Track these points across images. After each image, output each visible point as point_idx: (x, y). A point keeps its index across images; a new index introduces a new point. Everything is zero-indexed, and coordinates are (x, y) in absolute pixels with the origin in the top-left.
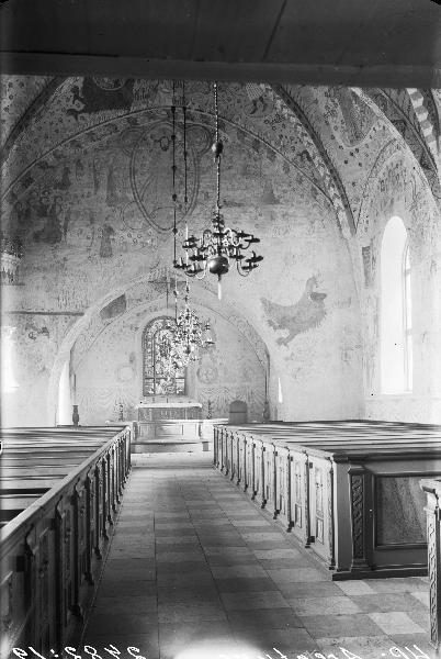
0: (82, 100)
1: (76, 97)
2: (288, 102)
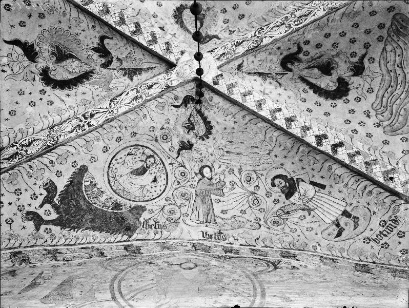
0: (55, 207)
1: (48, 200)
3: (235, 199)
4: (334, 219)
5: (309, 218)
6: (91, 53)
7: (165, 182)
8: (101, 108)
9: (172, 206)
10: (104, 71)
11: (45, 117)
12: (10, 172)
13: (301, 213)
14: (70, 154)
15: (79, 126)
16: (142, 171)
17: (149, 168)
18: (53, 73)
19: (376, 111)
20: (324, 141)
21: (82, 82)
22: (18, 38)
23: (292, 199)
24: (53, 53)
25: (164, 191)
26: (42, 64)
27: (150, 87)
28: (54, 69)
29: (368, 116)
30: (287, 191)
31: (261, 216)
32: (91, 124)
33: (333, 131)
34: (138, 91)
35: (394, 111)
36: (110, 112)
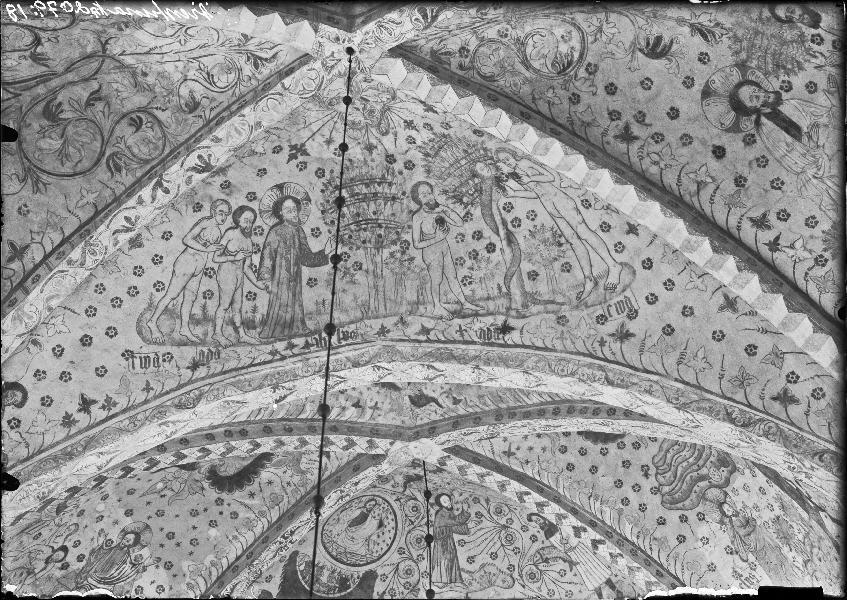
2: (659, 574)
3: (483, 538)
4: (597, 585)
5: (569, 576)
7: (393, 524)
9: (408, 562)
11: (235, 538)
13: (561, 565)
16: (362, 519)
17: (370, 511)
18: (223, 469)
19: (657, 468)
20: (582, 534)
21: (263, 466)
23: (552, 539)
25: (395, 538)
27: (356, 484)
29: (646, 475)
30: (546, 528)
31: (515, 560)
33: (598, 504)
35: (678, 474)
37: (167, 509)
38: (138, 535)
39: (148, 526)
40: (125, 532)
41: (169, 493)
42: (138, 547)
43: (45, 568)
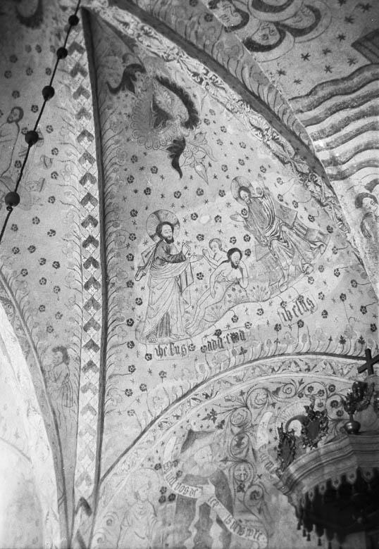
6: (138, 90)
8: (182, 68)
10: (148, 68)
12: (298, 134)
14: (253, 72)
15: (213, 83)
18: (183, 116)
22: (171, 167)
24: (164, 125)
26: (182, 131)
27: (126, 24)
28: (179, 118)
32: (205, 72)
34: (139, 36)
36: (181, 56)
37: (221, 163)
38: (242, 188)
39: (235, 179)
40: (239, 198)
41: (207, 160)
42: (251, 189)
43: (241, 270)
